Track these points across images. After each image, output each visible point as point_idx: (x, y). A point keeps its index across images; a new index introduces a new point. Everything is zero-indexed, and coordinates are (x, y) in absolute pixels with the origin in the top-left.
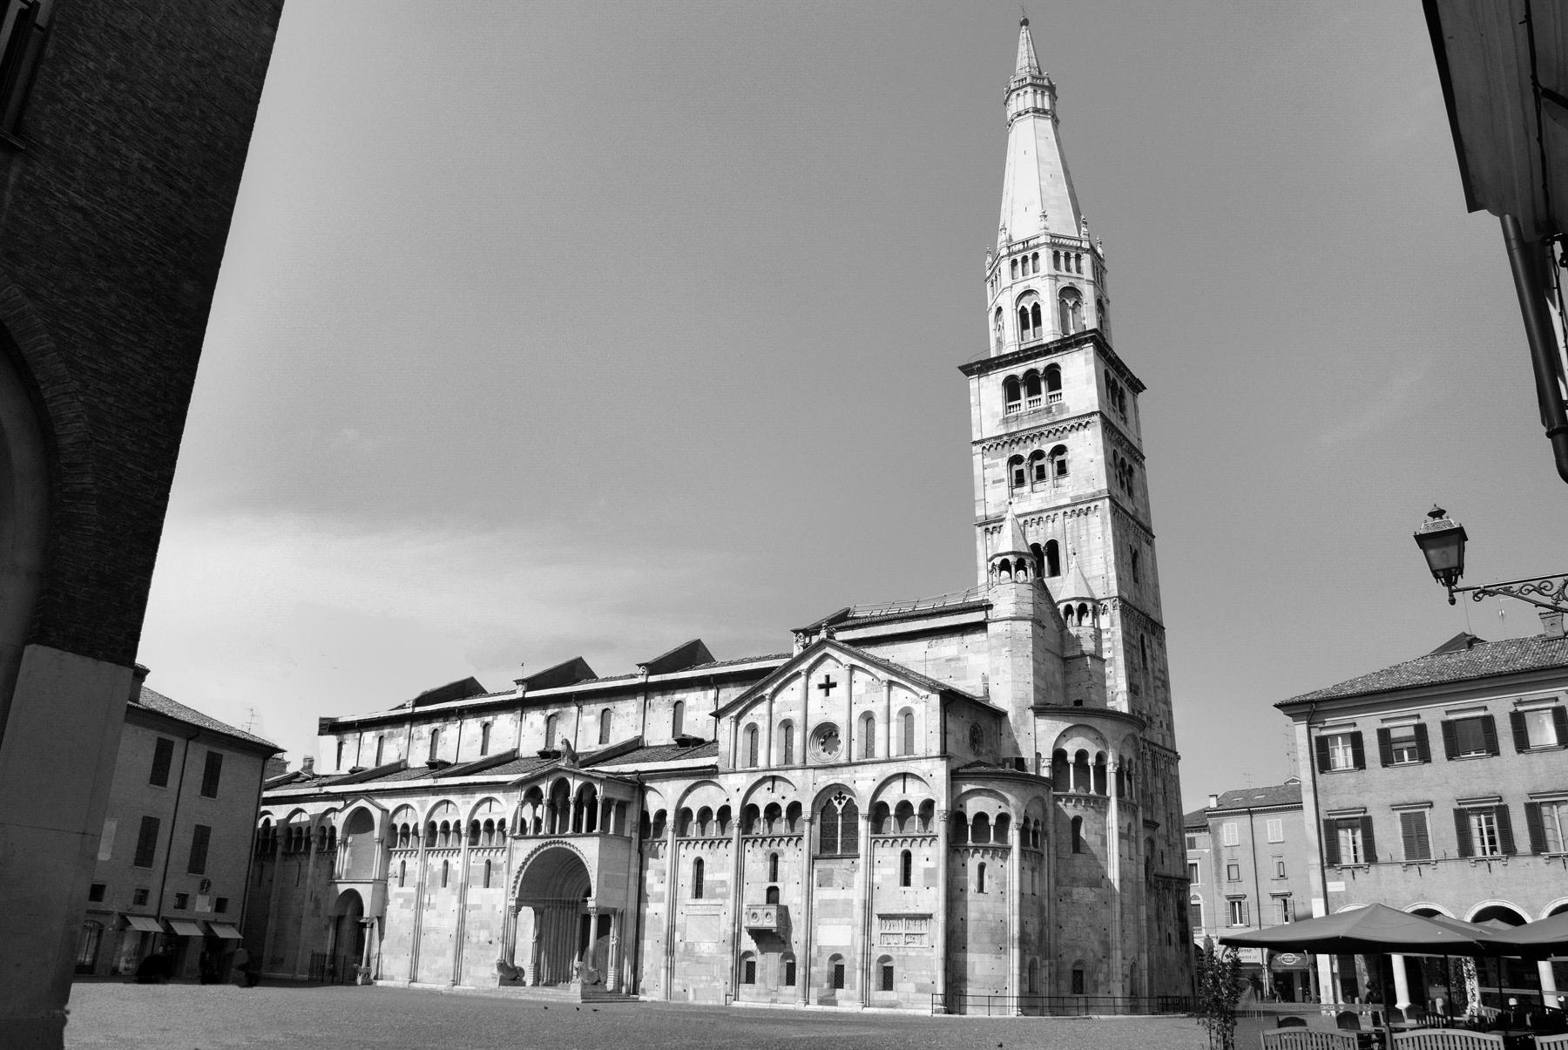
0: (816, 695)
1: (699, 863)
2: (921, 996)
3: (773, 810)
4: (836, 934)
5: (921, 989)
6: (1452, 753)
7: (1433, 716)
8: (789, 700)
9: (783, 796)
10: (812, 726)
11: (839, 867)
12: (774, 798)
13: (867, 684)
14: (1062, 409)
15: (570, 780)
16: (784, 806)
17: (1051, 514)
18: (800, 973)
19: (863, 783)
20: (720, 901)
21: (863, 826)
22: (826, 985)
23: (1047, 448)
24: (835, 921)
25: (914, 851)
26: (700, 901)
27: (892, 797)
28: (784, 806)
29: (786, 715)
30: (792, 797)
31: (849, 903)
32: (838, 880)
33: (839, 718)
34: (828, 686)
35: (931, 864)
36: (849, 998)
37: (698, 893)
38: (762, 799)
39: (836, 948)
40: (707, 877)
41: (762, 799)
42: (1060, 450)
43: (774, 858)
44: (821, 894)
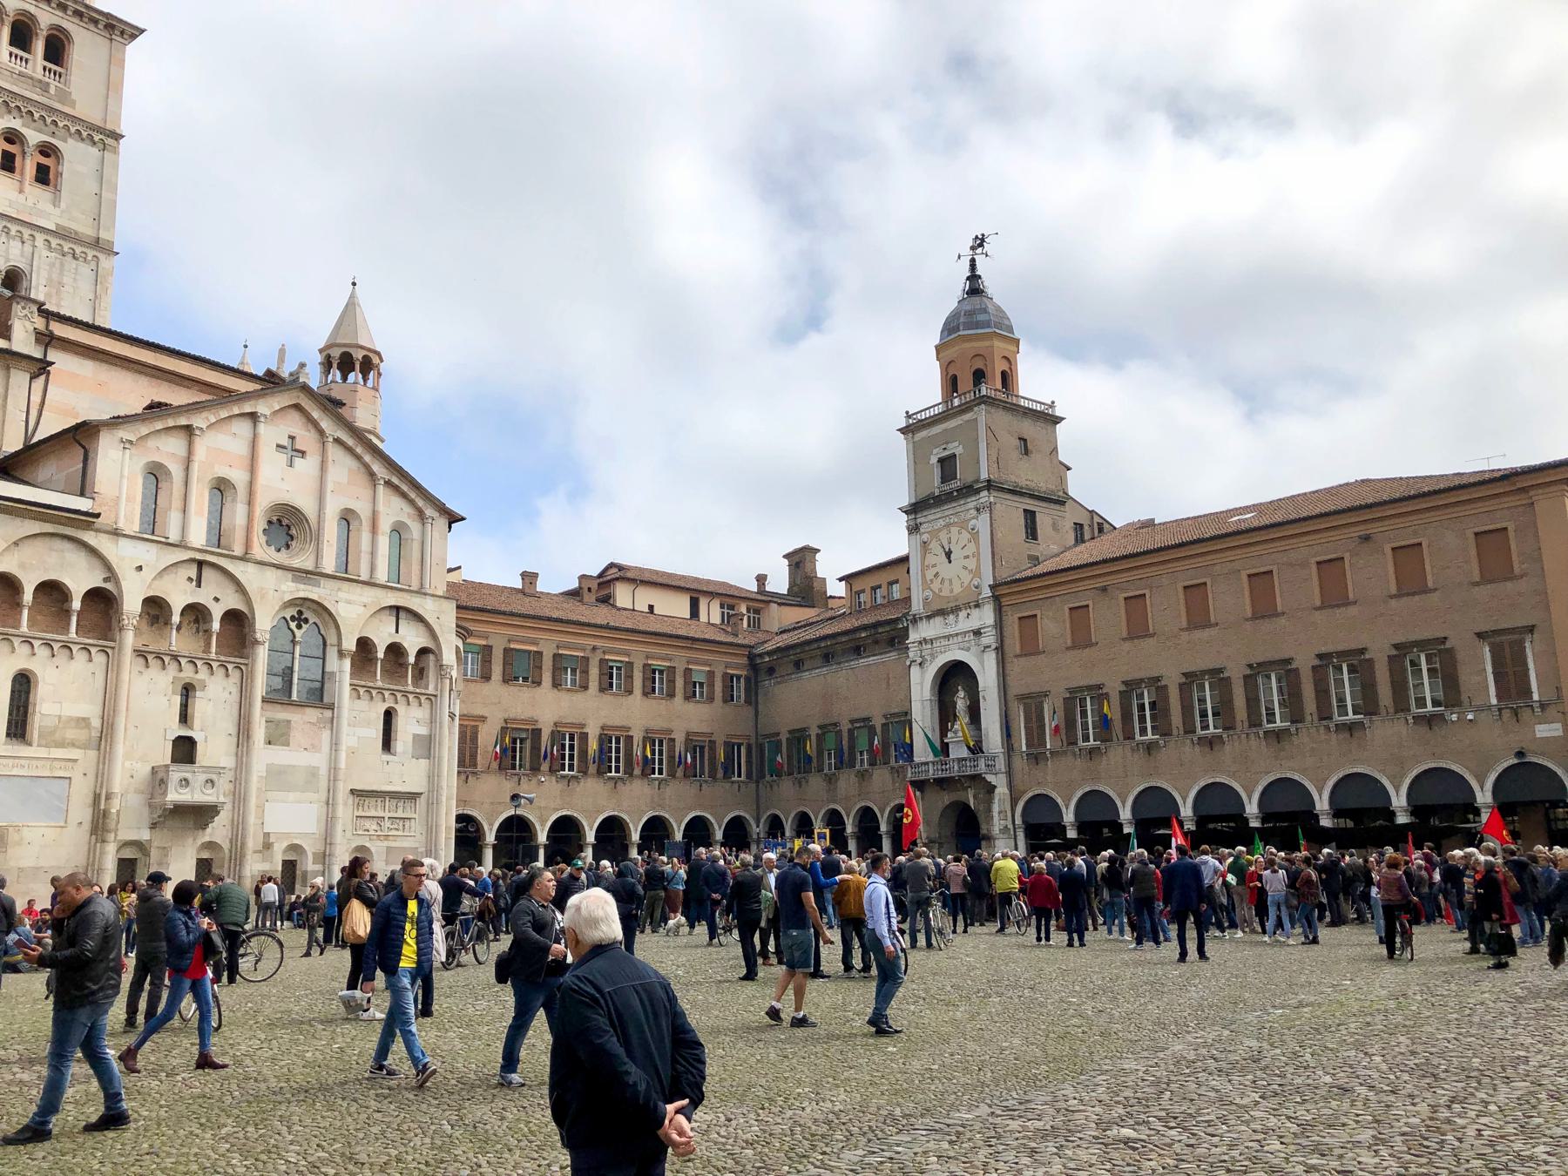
1: (23, 684)
3: (196, 614)
6: (508, 679)
7: (547, 645)
8: (220, 447)
9: (218, 599)
10: (263, 503)
11: (302, 720)
12: (203, 597)
14: (64, 96)
16: (217, 612)
17: (26, 232)
23: (34, 137)
24: (292, 796)
25: (401, 709)
28: (217, 612)
30: (232, 601)
31: (313, 773)
32: (296, 736)
33: (307, 505)
34: (294, 451)
35: (423, 731)
38: (179, 596)
41: (179, 596)
42: (46, 150)
43: (188, 691)
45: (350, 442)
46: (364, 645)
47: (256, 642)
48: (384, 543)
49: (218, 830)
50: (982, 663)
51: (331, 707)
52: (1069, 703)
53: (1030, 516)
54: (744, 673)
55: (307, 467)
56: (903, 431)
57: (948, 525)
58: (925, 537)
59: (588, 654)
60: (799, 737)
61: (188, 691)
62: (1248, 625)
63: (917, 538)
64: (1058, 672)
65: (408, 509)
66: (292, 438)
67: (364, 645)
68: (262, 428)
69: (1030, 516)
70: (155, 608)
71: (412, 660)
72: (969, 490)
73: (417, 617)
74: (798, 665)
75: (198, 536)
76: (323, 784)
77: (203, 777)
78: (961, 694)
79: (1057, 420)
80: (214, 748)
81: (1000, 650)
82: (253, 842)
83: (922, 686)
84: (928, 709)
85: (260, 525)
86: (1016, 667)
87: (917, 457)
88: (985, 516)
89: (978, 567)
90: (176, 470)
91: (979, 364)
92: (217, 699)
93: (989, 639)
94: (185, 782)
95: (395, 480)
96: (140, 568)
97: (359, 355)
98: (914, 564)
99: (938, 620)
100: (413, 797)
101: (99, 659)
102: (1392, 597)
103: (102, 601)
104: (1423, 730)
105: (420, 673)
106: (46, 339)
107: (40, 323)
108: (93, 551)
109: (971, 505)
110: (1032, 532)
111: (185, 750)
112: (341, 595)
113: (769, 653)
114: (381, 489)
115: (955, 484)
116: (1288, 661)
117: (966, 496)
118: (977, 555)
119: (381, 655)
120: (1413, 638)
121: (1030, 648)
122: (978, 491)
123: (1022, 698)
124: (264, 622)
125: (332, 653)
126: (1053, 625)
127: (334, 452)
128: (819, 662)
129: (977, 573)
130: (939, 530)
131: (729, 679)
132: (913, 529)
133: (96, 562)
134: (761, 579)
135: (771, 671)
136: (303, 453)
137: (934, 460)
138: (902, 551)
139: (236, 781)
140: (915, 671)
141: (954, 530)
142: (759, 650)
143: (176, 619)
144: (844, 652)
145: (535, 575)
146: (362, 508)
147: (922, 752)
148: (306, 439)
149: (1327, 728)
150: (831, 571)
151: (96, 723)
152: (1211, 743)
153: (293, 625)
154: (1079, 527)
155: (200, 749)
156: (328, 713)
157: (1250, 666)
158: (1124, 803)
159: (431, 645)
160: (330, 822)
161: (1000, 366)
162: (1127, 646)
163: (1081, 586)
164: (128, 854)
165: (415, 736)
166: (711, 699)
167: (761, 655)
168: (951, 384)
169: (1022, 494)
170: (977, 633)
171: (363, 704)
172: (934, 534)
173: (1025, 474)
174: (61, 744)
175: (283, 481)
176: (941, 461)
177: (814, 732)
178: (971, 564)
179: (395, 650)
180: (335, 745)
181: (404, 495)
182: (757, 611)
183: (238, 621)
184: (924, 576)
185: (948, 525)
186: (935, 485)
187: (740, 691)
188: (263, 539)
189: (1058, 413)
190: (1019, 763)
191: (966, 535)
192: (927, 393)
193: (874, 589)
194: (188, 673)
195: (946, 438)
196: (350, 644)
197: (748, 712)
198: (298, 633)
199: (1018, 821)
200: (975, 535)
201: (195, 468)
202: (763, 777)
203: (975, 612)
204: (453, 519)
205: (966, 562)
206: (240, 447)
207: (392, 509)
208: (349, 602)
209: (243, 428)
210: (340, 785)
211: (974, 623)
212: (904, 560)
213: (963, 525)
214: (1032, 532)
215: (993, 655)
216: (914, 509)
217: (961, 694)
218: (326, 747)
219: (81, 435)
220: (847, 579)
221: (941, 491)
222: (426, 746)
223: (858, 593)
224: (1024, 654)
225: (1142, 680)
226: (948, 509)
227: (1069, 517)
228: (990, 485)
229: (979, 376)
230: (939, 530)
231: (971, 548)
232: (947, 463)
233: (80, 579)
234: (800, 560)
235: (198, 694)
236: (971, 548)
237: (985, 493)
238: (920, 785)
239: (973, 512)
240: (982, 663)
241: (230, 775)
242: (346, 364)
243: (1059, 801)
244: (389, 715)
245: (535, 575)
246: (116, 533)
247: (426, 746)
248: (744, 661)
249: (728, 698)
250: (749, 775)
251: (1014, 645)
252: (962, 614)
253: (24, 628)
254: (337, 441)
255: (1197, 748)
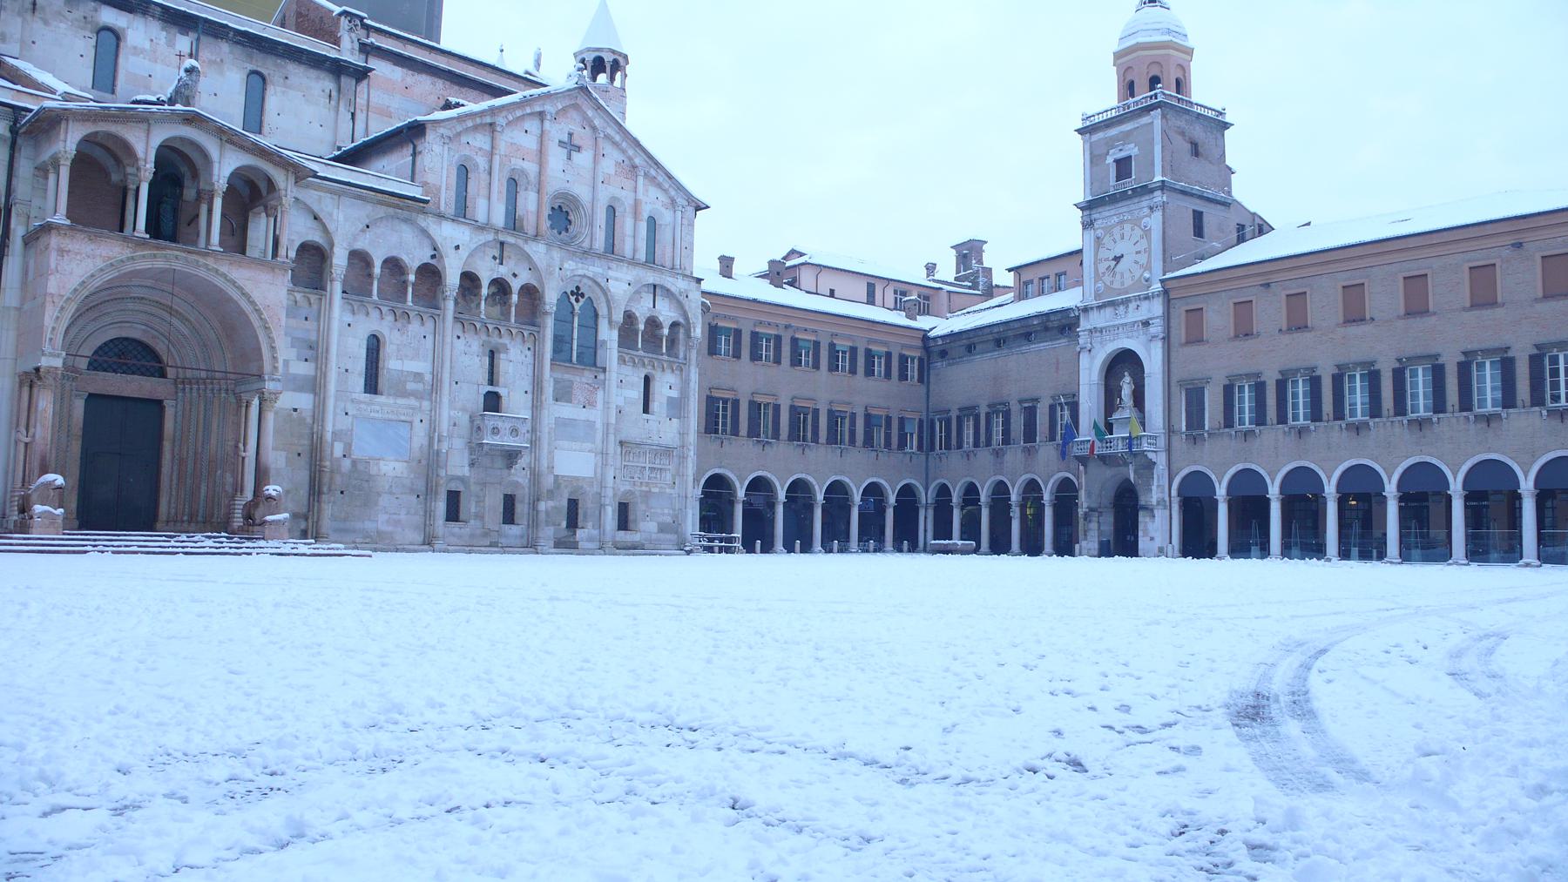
0: (556, 157)
2: (662, 536)
4: (573, 462)
5: (663, 529)
11: (581, 379)
12: (503, 271)
13: (617, 164)
15: (211, 145)
18: (521, 509)
19: (620, 284)
20: (413, 402)
21: (609, 335)
22: (564, 524)
24: (575, 445)
26: (378, 399)
27: (642, 310)
28: (515, 285)
29: (517, 163)
30: (525, 277)
31: (590, 425)
32: (579, 395)
33: (582, 191)
34: (571, 146)
35: (674, 394)
36: (590, 539)
37: (372, 386)
39: (577, 478)
40: (392, 363)
44: (555, 411)
45: (618, 138)
46: (629, 317)
47: (546, 313)
48: (643, 227)
49: (519, 475)
50: (1148, 351)
51: (604, 370)
52: (1228, 391)
53: (1198, 217)
54: (917, 354)
55: (583, 159)
56: (1079, 131)
57: (1121, 222)
58: (1099, 232)
59: (781, 332)
60: (969, 411)
61: (492, 354)
62: (1400, 323)
63: (1091, 234)
64: (1218, 361)
65: (663, 198)
66: (571, 135)
67: (629, 317)
68: (547, 124)
69: (1198, 217)
70: (470, 280)
71: (666, 331)
72: (1145, 190)
73: (668, 293)
74: (970, 349)
75: (499, 219)
76: (599, 436)
77: (508, 425)
78: (1127, 379)
79: (1226, 126)
80: (516, 402)
81: (1167, 340)
82: (548, 482)
83: (1090, 372)
84: (1095, 388)
85: (546, 211)
86: (1182, 354)
87: (1094, 159)
88: (1158, 215)
89: (1149, 262)
90: (482, 162)
91: (1155, 71)
92: (516, 363)
93: (1157, 328)
94: (496, 431)
95: (653, 172)
96: (457, 247)
97: (608, 58)
98: (1088, 258)
99: (1109, 311)
100: (667, 451)
101: (429, 324)
102: (1536, 300)
103: (431, 273)
104: (1556, 423)
105: (672, 342)
106: (366, 49)
107: (362, 33)
108: (424, 232)
109: (1145, 204)
110: (1199, 231)
111: (493, 402)
112: (611, 273)
113: (943, 337)
114: (641, 180)
115: (1130, 183)
116: (1436, 356)
117: (1142, 195)
118: (1148, 251)
119: (642, 327)
120: (1553, 338)
121: (1195, 338)
122: (1152, 191)
123: (1181, 383)
124: (551, 297)
125: (603, 325)
126: (1218, 318)
127: (608, 149)
128: (991, 345)
129: (1148, 267)
130: (1112, 227)
131: (903, 360)
132: (1087, 225)
133: (426, 242)
134: (931, 268)
135: (943, 354)
136: (579, 149)
137: (1110, 160)
138: (1078, 247)
139: (534, 430)
140: (1084, 360)
141: (1127, 227)
142: (932, 334)
143: (485, 291)
144: (1016, 337)
145: (732, 259)
146: (627, 197)
147: (1085, 433)
148: (582, 136)
149: (1467, 418)
150: (999, 264)
151: (428, 377)
152: (1358, 428)
153: (573, 299)
154: (1241, 227)
155: (504, 402)
156: (601, 376)
157: (1399, 360)
158: (1273, 481)
159: (681, 320)
160: (604, 465)
161: (1174, 74)
162: (1286, 339)
163: (1247, 283)
164: (453, 487)
165: (670, 399)
166: (888, 375)
167: (935, 338)
168: (1129, 89)
169: (1192, 195)
170: (1146, 324)
171: (627, 370)
172: (1108, 230)
173: (1196, 176)
174: (404, 394)
175: (566, 174)
176: (1117, 161)
177: (983, 411)
178: (1143, 259)
179: (653, 323)
180: (606, 403)
181: (659, 186)
182: (927, 298)
183: (531, 293)
184: (1096, 269)
185: (1121, 222)
186: (1112, 185)
187: (913, 370)
188: (549, 223)
189: (1227, 119)
190: (1179, 443)
191: (1138, 232)
192: (1104, 97)
193: (1042, 279)
194: (495, 339)
195: (1126, 137)
196: (619, 317)
197: (923, 389)
198: (577, 306)
199: (1174, 493)
200: (1147, 233)
201: (497, 159)
202: (932, 448)
203: (1145, 305)
204: (700, 207)
205: (1138, 258)
206: (530, 142)
207: (652, 200)
208: (616, 279)
209: (533, 125)
210: (612, 437)
211: (1142, 315)
212: (1080, 252)
213: (1136, 222)
214: (1199, 231)
215: (1160, 344)
216: (1088, 207)
217: (1127, 379)
218: (600, 405)
219: (413, 133)
220: (1016, 270)
221: (1113, 190)
222: (677, 407)
223: (1026, 284)
224: (1188, 343)
225: (1298, 370)
226: (1123, 208)
227: (1234, 219)
228: (1163, 186)
229: (1154, 81)
230: (1112, 227)
231: (1143, 244)
232: (1123, 167)
233: (415, 257)
234: (968, 253)
235: (502, 356)
236: (1143, 244)
237: (1158, 193)
238: (1083, 460)
239: (1146, 211)
240: (1148, 351)
241: (528, 426)
242: (598, 66)
243: (1213, 477)
244: (647, 380)
245: (732, 259)
246: (441, 216)
247: (677, 407)
248: (919, 343)
249: (903, 376)
250: (920, 447)
251: (1179, 333)
252: (1132, 306)
253: (375, 297)
254: (607, 137)
255: (1345, 433)
